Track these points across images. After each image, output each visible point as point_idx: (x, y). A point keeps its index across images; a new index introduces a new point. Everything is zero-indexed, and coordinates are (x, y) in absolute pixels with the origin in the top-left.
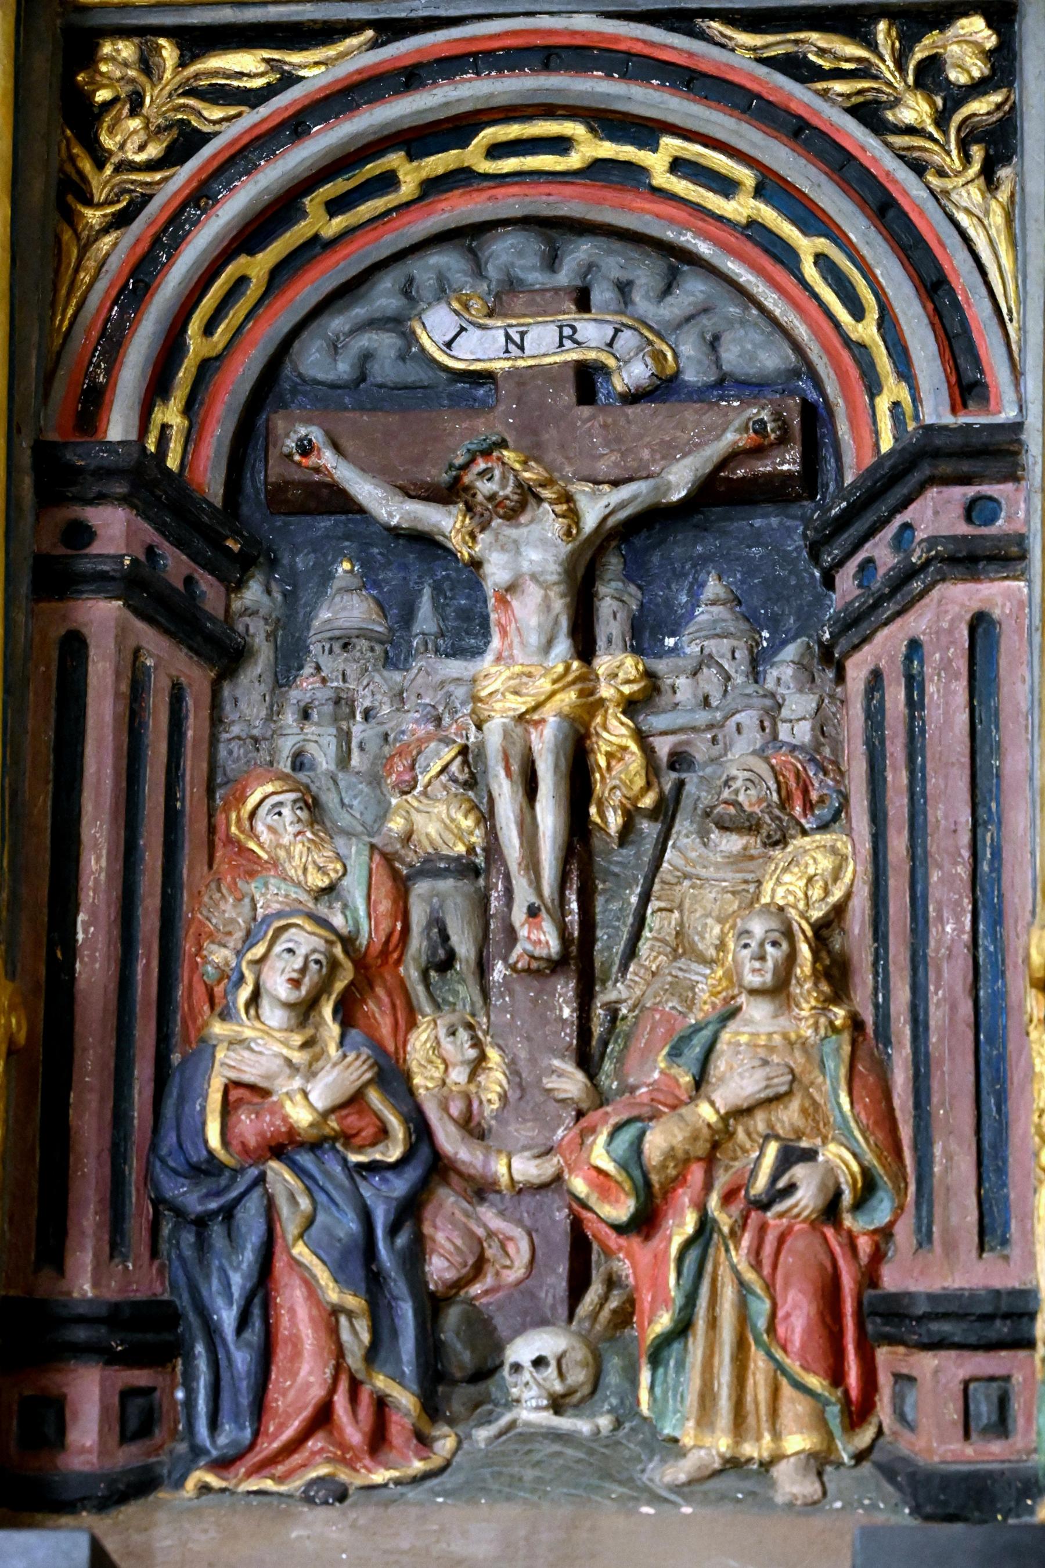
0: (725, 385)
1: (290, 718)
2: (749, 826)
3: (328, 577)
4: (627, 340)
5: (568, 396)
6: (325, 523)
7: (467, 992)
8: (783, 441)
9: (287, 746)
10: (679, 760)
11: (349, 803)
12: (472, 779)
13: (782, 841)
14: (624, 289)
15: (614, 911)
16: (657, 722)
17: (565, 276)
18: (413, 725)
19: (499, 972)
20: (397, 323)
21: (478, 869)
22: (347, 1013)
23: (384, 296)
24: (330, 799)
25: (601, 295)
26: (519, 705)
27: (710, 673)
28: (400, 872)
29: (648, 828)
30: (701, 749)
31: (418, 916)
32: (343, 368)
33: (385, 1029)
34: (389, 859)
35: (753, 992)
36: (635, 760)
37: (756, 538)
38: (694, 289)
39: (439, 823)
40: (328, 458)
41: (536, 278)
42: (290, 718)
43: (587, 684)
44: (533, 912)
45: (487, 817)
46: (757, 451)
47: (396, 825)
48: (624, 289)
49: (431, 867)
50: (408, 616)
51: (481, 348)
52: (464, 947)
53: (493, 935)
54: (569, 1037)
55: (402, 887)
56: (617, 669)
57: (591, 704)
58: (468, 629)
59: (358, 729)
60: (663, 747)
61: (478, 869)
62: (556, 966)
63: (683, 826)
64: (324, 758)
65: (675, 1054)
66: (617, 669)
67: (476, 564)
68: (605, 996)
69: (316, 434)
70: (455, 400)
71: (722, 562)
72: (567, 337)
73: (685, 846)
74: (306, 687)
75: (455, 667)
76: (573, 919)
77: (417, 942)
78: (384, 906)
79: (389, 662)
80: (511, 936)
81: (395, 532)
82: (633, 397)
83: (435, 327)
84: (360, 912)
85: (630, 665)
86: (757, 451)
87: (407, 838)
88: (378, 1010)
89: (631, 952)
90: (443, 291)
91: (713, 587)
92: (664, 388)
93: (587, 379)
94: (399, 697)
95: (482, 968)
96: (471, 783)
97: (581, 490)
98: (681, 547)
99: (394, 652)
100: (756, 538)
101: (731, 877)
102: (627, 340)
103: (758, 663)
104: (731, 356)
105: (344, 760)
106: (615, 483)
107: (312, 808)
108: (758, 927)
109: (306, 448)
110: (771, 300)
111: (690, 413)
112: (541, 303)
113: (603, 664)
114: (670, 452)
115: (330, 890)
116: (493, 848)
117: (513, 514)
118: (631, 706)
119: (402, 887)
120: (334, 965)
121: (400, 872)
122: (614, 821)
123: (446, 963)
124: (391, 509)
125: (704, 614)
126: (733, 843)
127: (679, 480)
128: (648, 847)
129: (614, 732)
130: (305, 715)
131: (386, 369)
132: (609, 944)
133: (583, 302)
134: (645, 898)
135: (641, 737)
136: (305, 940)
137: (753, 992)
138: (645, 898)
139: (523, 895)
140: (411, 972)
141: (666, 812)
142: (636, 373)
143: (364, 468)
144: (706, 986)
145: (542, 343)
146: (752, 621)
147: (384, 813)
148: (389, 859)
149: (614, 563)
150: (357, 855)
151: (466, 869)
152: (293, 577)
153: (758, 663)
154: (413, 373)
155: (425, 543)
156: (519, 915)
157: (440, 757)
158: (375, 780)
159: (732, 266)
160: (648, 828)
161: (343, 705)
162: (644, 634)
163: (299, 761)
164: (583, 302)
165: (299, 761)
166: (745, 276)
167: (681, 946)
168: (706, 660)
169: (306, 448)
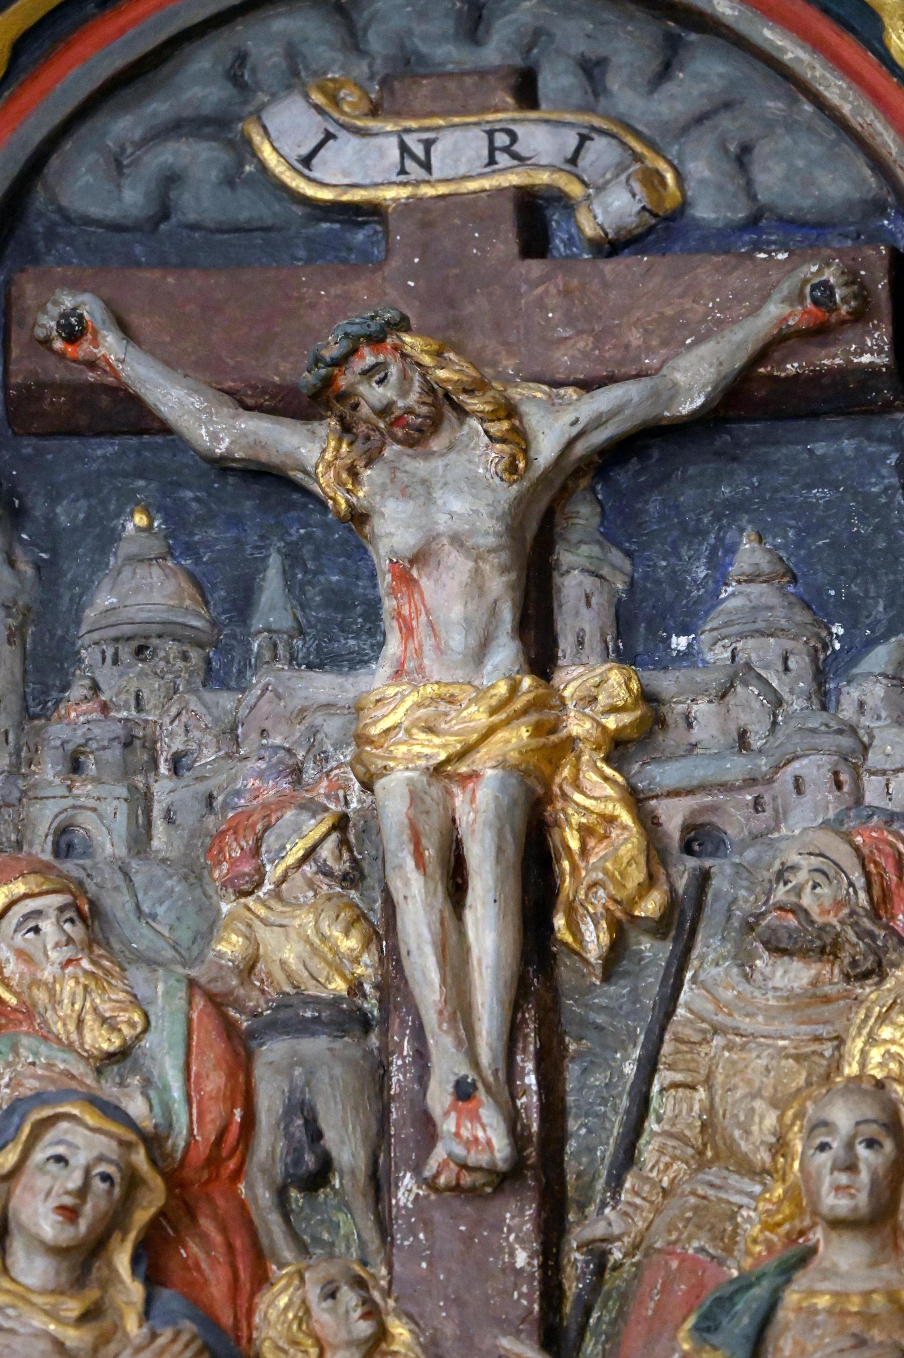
0: (759, 224)
1: (49, 771)
2: (826, 948)
3: (109, 538)
4: (600, 151)
5: (506, 243)
6: (104, 449)
7: (354, 1225)
8: (860, 316)
9: (45, 817)
10: (700, 837)
11: (151, 912)
12: (355, 868)
13: (877, 972)
14: (592, 70)
15: (597, 1087)
16: (666, 775)
17: (496, 51)
18: (256, 782)
19: (406, 1190)
20: (223, 127)
21: (370, 1018)
22: (152, 1262)
23: (198, 84)
24: (118, 904)
25: (555, 80)
26: (434, 749)
27: (747, 694)
28: (235, 1023)
29: (652, 950)
30: (735, 820)
31: (269, 1099)
32: (133, 199)
33: (217, 1288)
34: (218, 1002)
35: (837, 1224)
36: (627, 839)
37: (820, 472)
38: (707, 72)
39: (300, 942)
40: (110, 346)
41: (449, 53)
42: (49, 771)
43: (545, 713)
44: (464, 1092)
45: (384, 932)
46: (820, 333)
47: (230, 946)
48: (592, 70)
49: (292, 1016)
50: (243, 602)
51: (359, 167)
52: (347, 1148)
53: (396, 1130)
54: (526, 1299)
55: (240, 1049)
56: (594, 689)
57: (554, 748)
58: (346, 620)
59: (163, 789)
60: (673, 816)
61: (370, 1018)
62: (504, 1180)
63: (709, 947)
64: (107, 836)
65: (707, 1327)
66: (594, 689)
67: (359, 518)
68: (584, 1229)
69: (90, 307)
70: (318, 250)
71: (765, 512)
72: (502, 148)
73: (713, 980)
74: (76, 719)
75: (323, 686)
76: (530, 1100)
77: (268, 1143)
78: (214, 1082)
79: (213, 677)
80: (427, 1129)
81: (222, 466)
82: (612, 247)
83: (283, 136)
84: (173, 1090)
85: (616, 683)
86: (820, 333)
87: (249, 967)
88: (203, 1254)
89: (627, 1157)
90: (295, 75)
91: (749, 553)
92: (660, 231)
93: (534, 218)
94: (230, 734)
95: (379, 1184)
96: (353, 878)
97: (530, 397)
98: (697, 486)
99: (222, 661)
100: (820, 472)
101: (792, 1032)
102: (600, 151)
103: (826, 675)
104: (771, 179)
105: (140, 839)
106: (587, 385)
107: (89, 918)
108: (843, 1116)
109: (74, 331)
110: (835, 90)
111: (706, 270)
112: (458, 96)
113: (571, 680)
114: (676, 335)
115: (121, 1056)
116: (394, 982)
117: (418, 435)
118: (618, 749)
119: (240, 1049)
120: (133, 1182)
121: (237, 1024)
122: (595, 940)
123: (314, 1176)
124: (212, 426)
125: (734, 598)
126: (795, 975)
127: (692, 380)
128: (652, 982)
129: (592, 792)
130: (75, 765)
131: (201, 201)
132: (589, 1142)
133: (526, 92)
134: (649, 1066)
135: (636, 799)
136: (84, 1142)
137: (837, 1224)
138: (649, 1066)
139: (447, 1064)
140: (259, 1193)
141: (681, 923)
142: (617, 206)
143: (171, 363)
144: (756, 1209)
145: (462, 159)
146: (816, 607)
147: (209, 931)
148: (218, 1002)
149: (584, 515)
150: (165, 996)
151: (346, 1019)
152: (51, 538)
153: (826, 675)
154: (247, 207)
155: (271, 482)
156: (439, 1097)
157: (300, 835)
158: (193, 874)
159: (771, 36)
160: (652, 950)
161: (137, 748)
162: (635, 632)
163: (65, 841)
164: (526, 92)
165: (65, 841)
166: (792, 52)
167: (712, 1145)
168: (743, 671)
169: (74, 331)
